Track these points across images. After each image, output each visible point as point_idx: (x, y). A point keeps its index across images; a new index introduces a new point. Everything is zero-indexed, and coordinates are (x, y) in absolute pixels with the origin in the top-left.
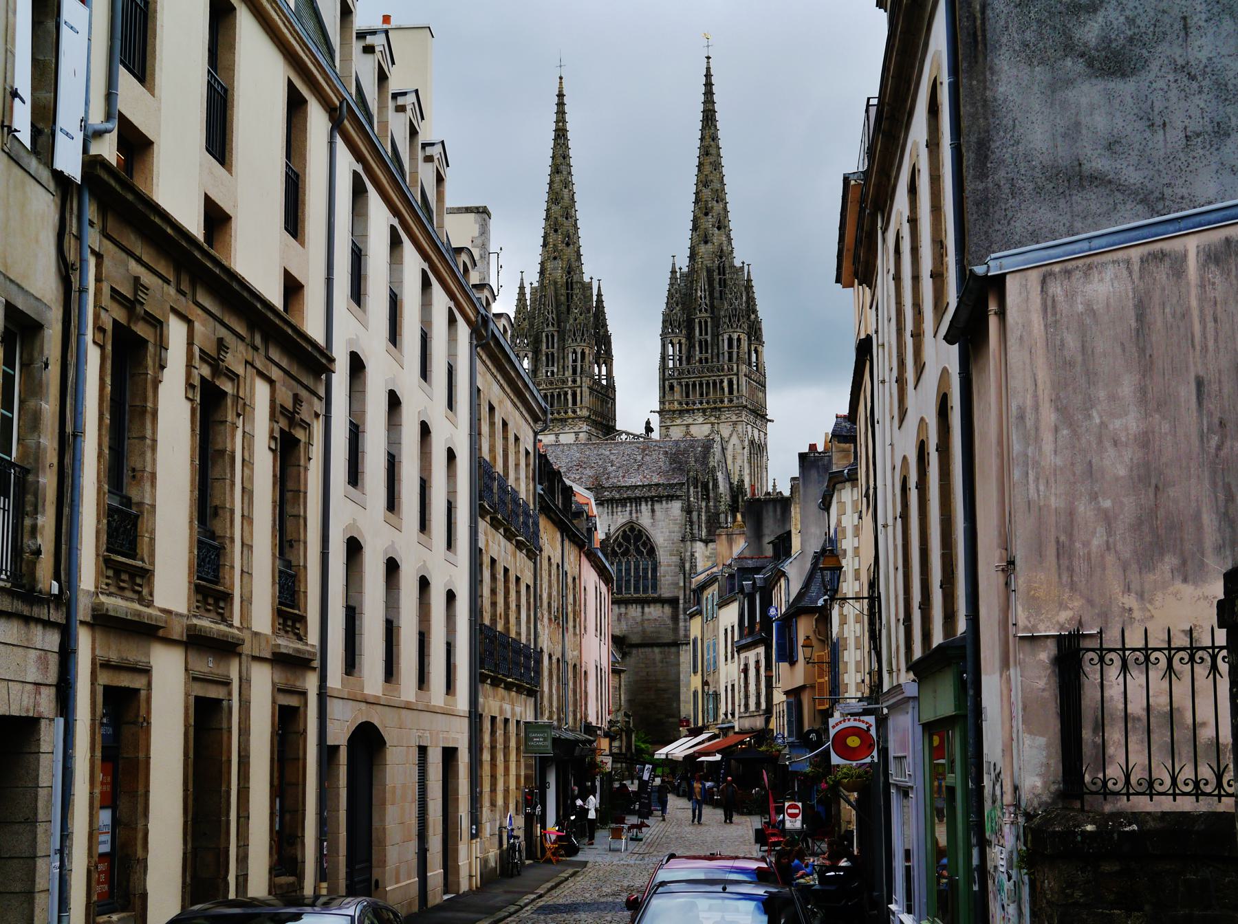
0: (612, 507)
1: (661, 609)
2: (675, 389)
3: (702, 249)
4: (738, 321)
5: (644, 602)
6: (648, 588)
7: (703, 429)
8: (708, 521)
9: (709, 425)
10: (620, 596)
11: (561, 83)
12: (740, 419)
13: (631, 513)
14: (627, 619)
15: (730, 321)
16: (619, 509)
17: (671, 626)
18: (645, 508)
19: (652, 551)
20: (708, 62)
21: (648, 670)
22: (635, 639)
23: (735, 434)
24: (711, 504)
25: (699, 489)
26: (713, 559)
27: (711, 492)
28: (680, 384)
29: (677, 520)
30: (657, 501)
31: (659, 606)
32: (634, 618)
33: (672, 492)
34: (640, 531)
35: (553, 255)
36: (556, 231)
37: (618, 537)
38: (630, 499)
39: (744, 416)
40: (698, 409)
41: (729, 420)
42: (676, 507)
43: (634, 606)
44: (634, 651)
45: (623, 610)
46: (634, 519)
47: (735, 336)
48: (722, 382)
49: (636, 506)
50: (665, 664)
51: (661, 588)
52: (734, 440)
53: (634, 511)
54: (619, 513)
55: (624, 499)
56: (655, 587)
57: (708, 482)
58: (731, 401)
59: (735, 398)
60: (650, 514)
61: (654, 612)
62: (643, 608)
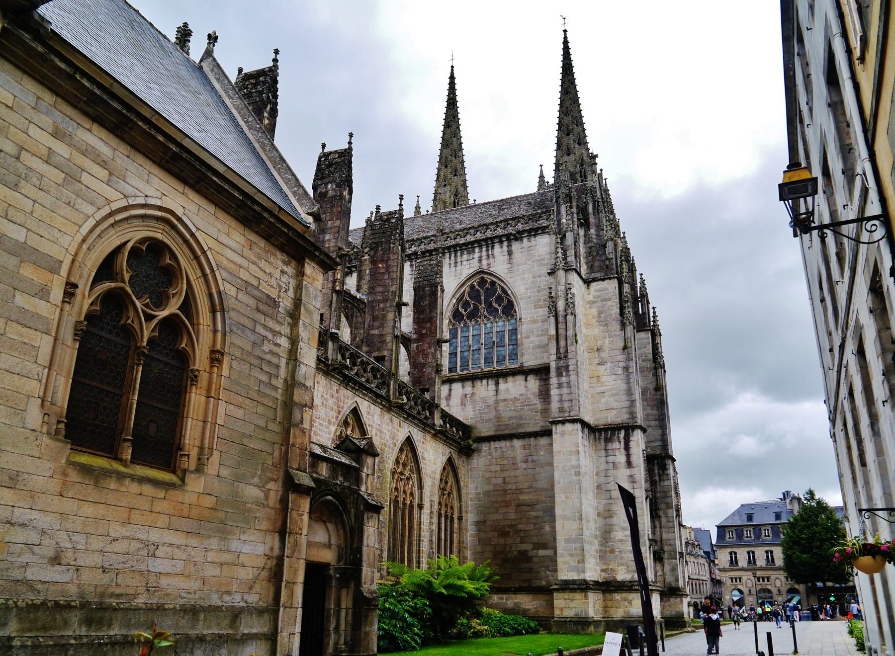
0: (456, 256)
1: (523, 383)
5: (498, 376)
6: (504, 357)
8: (589, 254)
10: (465, 372)
11: (452, 70)
13: (480, 261)
14: (474, 402)
16: (465, 257)
17: (539, 406)
18: (499, 251)
19: (509, 309)
20: (565, 34)
21: (505, 474)
22: (485, 430)
24: (592, 231)
25: (575, 210)
26: (599, 304)
27: (591, 216)
29: (544, 259)
30: (516, 239)
31: (520, 378)
32: (484, 400)
33: (536, 225)
34: (493, 283)
35: (443, 184)
36: (446, 167)
37: (463, 294)
38: (478, 241)
42: (544, 244)
43: (485, 381)
44: (485, 447)
45: (468, 389)
46: (485, 267)
49: (487, 250)
50: (530, 465)
51: (522, 355)
53: (484, 257)
54: (464, 263)
55: (472, 243)
56: (514, 356)
57: (587, 204)
60: (507, 257)
61: (513, 388)
62: (497, 384)
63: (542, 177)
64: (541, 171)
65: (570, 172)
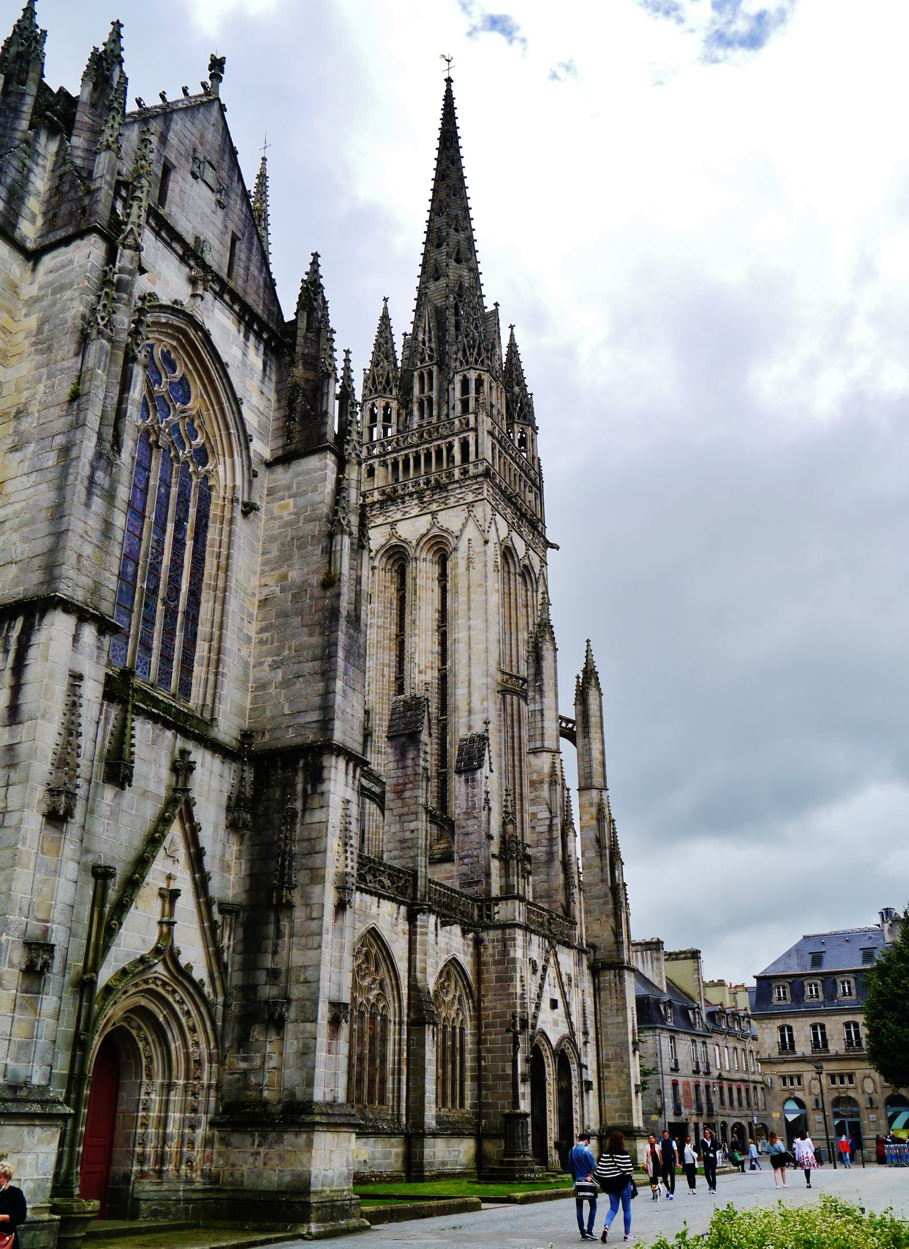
2: (376, 472)
3: (432, 285)
4: (479, 354)
7: (418, 524)
9: (429, 517)
12: (480, 497)
15: (464, 355)
23: (471, 523)
28: (384, 464)
39: (485, 492)
40: (411, 495)
41: (462, 502)
47: (473, 375)
48: (450, 447)
52: (471, 532)
58: (465, 472)
59: (471, 466)
63: (385, 319)
64: (386, 308)
65: (436, 307)
